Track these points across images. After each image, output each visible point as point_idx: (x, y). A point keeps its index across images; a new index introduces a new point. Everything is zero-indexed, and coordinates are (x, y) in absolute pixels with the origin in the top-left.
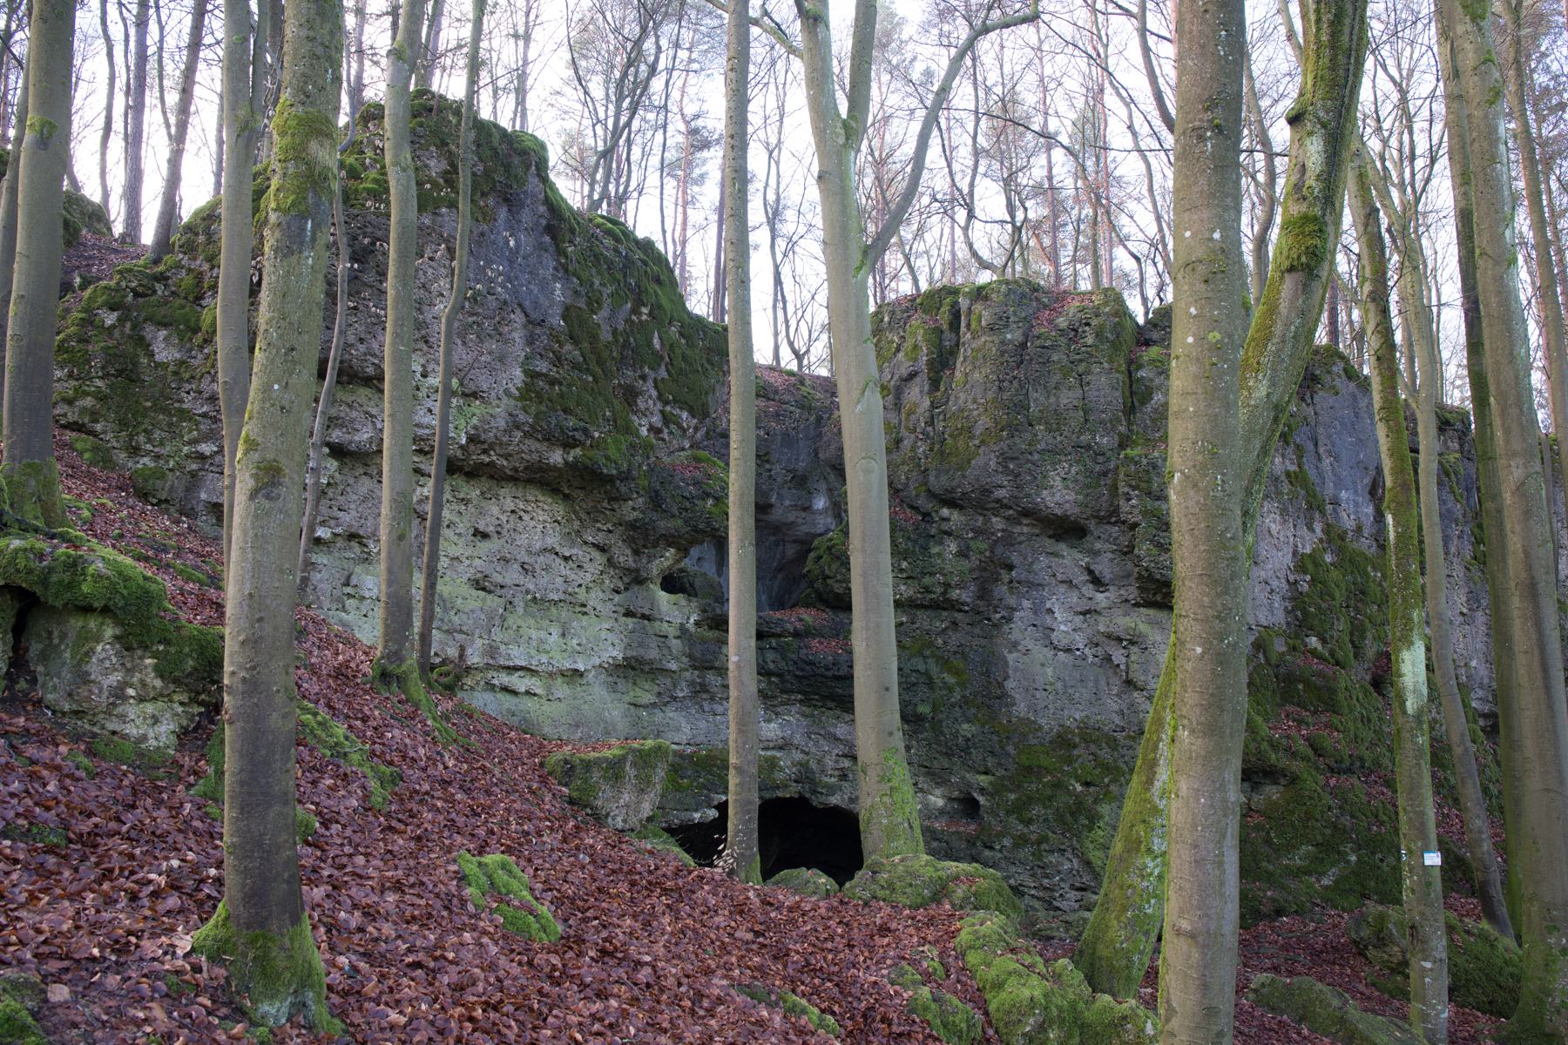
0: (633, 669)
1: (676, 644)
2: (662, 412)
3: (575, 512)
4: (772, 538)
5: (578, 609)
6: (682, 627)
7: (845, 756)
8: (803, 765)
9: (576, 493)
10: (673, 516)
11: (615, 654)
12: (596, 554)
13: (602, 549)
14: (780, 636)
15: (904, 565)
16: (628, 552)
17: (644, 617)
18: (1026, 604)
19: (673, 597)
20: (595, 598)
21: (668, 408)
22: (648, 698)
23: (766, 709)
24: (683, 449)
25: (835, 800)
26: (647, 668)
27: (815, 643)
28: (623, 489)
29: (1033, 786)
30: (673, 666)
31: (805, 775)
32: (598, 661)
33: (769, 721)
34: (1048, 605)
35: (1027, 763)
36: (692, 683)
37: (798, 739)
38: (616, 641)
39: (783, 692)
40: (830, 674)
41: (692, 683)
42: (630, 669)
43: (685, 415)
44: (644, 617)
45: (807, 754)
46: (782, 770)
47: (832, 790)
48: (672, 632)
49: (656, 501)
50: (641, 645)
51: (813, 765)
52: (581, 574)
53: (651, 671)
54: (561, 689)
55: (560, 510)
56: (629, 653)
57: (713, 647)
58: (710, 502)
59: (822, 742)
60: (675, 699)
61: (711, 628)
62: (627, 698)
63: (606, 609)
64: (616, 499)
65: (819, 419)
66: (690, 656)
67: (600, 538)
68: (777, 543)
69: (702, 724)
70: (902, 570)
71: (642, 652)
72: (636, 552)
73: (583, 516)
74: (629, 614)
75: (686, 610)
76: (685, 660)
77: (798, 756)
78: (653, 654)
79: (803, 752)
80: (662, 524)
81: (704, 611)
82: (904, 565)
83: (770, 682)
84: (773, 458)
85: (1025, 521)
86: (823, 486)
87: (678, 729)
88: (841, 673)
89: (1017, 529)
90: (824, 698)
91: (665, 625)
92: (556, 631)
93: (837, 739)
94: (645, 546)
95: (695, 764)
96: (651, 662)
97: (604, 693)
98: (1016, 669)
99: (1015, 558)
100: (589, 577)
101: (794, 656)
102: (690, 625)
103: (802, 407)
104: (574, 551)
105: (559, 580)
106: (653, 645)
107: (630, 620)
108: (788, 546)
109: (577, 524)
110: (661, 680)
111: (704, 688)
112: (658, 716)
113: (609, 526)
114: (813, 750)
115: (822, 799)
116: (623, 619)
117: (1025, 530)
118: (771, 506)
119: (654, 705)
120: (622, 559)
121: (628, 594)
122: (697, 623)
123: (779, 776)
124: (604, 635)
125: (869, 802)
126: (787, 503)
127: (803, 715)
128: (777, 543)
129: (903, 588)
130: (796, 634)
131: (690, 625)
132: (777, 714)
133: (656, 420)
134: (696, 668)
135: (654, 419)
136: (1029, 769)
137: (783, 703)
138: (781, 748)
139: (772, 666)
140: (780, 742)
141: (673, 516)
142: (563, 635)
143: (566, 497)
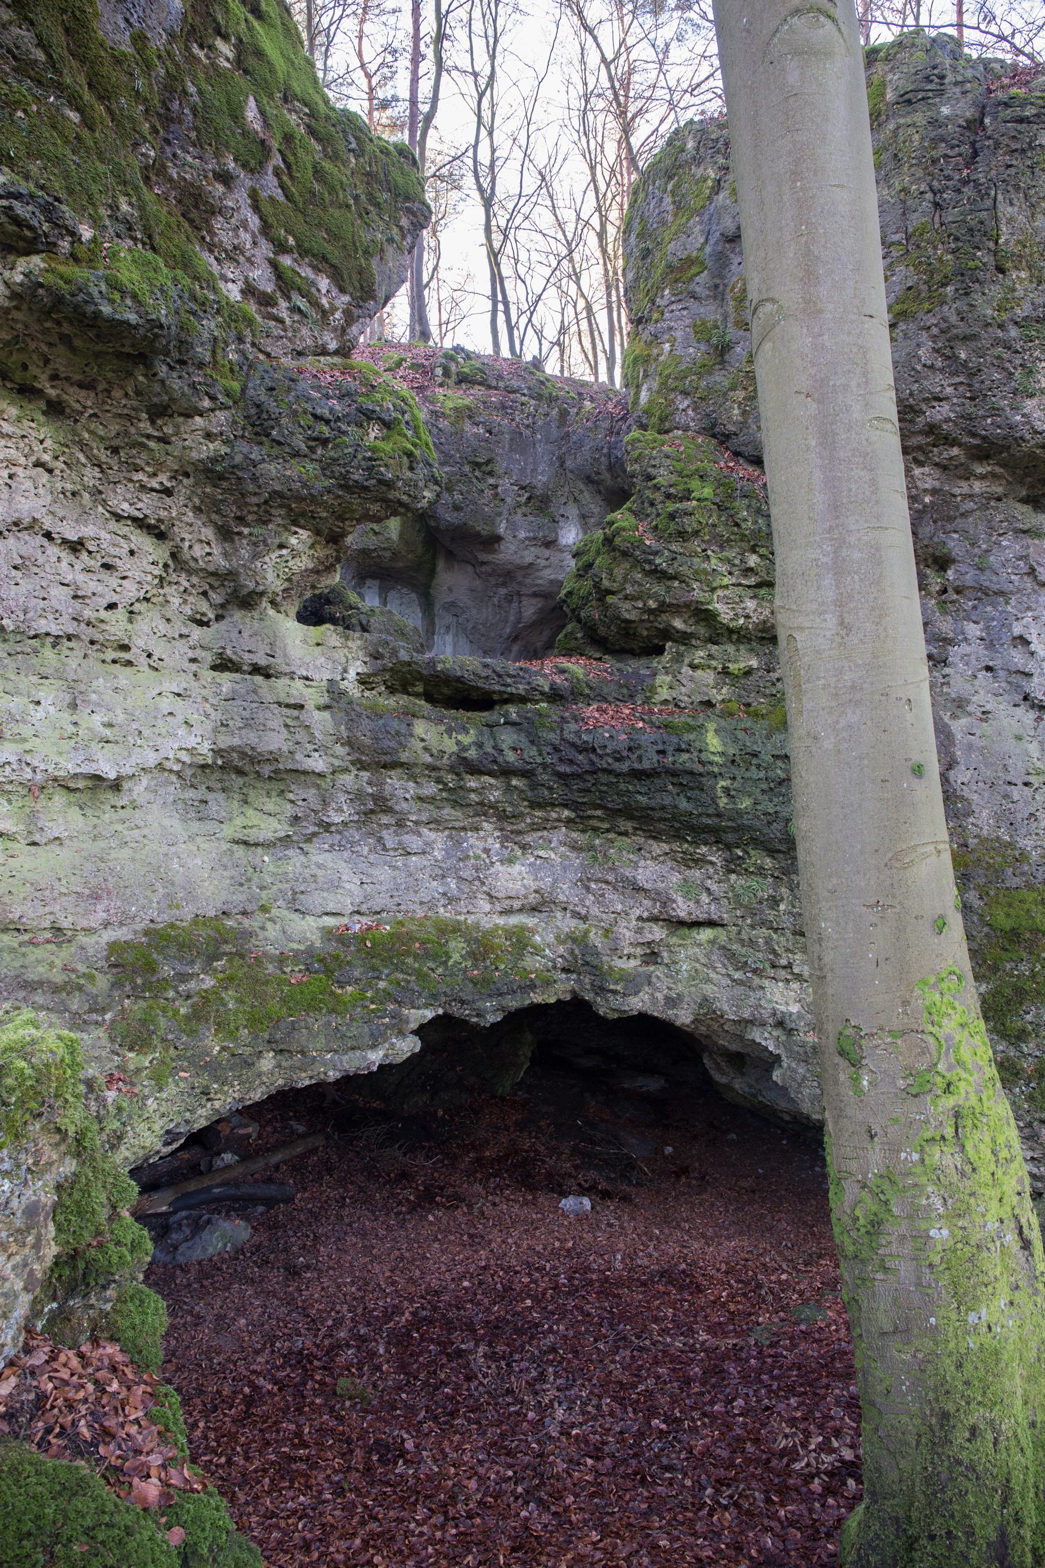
0: (240, 772)
1: (321, 721)
2: (274, 265)
3: (83, 446)
4: (503, 591)
5: (110, 654)
6: (333, 689)
7: (654, 919)
8: (578, 940)
9: (74, 397)
10: (296, 454)
11: (192, 742)
12: (141, 540)
13: (158, 533)
14: (523, 700)
15: (753, 560)
16: (208, 533)
17: (256, 670)
18: (973, 630)
19: (315, 632)
20: (146, 631)
21: (286, 261)
22: (270, 828)
23: (504, 839)
24: (324, 352)
25: (637, 1003)
26: (266, 770)
27: (590, 711)
28: (176, 384)
29: (1024, 968)
30: (318, 763)
31: (582, 960)
32: (152, 759)
33: (511, 861)
34: (1017, 630)
35: (1007, 924)
36: (358, 796)
37: (565, 892)
38: (194, 718)
39: (534, 805)
40: (624, 767)
41: (358, 796)
42: (234, 770)
43: (324, 283)
44: (256, 670)
45: (584, 918)
46: (538, 951)
47: (633, 983)
48: (312, 696)
49: (259, 425)
50: (248, 724)
51: (596, 938)
52: (114, 581)
53: (276, 776)
54: (61, 816)
55: (45, 437)
56: (225, 741)
57: (395, 724)
58: (374, 432)
59: (610, 895)
60: (327, 827)
61: (392, 690)
62: (229, 831)
63: (176, 655)
64: (159, 412)
65: (564, 414)
66: (349, 743)
67: (148, 506)
68: (509, 599)
69: (383, 874)
70: (748, 571)
71: (251, 737)
72: (226, 534)
73: (103, 456)
74: (224, 665)
75: (340, 655)
76: (340, 750)
77: (568, 924)
78: (275, 741)
79: (576, 915)
80: (272, 469)
81: (376, 656)
82: (753, 560)
83: (509, 789)
84: (500, 467)
85: (980, 470)
86: (572, 511)
87: (335, 886)
88: (646, 765)
89: (962, 488)
90: (613, 813)
91: (299, 684)
92: (50, 695)
93: (638, 889)
94: (241, 520)
95: (371, 954)
96: (273, 758)
97: (175, 824)
98: (970, 747)
99: (955, 545)
100: (131, 591)
101: (553, 737)
102: (350, 686)
103: (539, 397)
104: (88, 531)
105: (59, 595)
106: (275, 723)
107: (227, 681)
108: (525, 602)
109: (91, 476)
110: (297, 792)
111: (381, 805)
112: (295, 862)
113: (164, 478)
114: (595, 911)
115: (616, 1002)
116: (208, 675)
117: (978, 486)
118: (498, 539)
119: (286, 841)
120: (198, 551)
121: (222, 626)
122: (364, 681)
123: (532, 963)
124: (166, 704)
125: (875, 1158)
126: (522, 534)
127: (574, 847)
128: (509, 599)
129: (750, 604)
130: (555, 696)
131: (350, 686)
132: (524, 847)
133: (262, 277)
134: (363, 766)
135: (255, 274)
136: (1014, 935)
137: (534, 828)
138: (534, 909)
139: (511, 757)
140: (533, 899)
141: (296, 454)
142: (73, 706)
143: (55, 409)
